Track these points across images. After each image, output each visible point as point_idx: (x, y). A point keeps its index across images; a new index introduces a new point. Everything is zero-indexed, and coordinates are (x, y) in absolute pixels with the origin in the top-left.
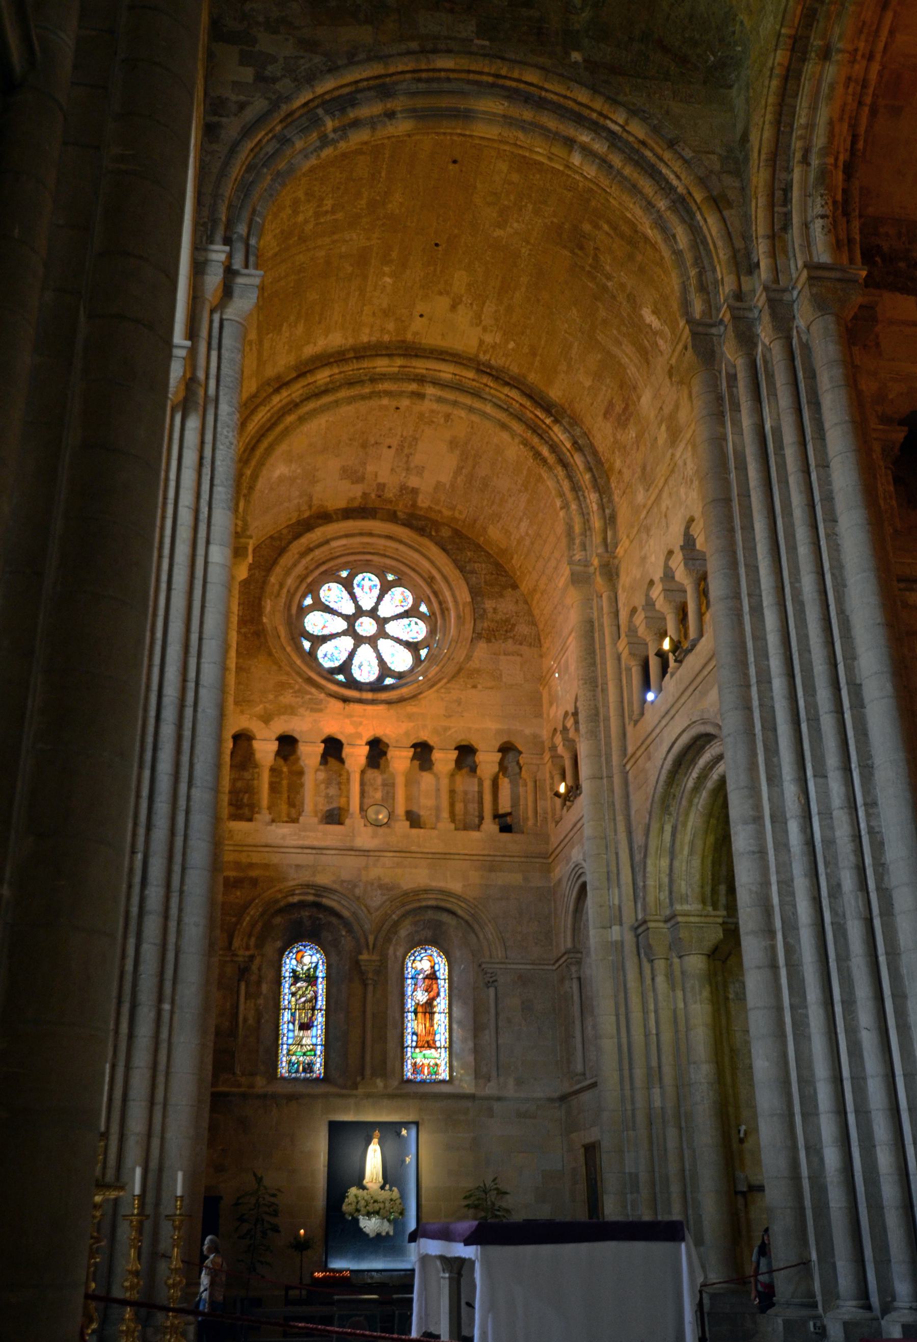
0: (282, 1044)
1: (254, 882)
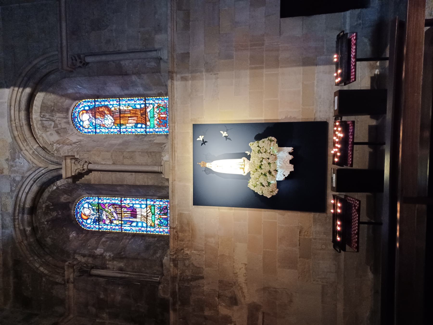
0: (147, 231)
1: (16, 262)
